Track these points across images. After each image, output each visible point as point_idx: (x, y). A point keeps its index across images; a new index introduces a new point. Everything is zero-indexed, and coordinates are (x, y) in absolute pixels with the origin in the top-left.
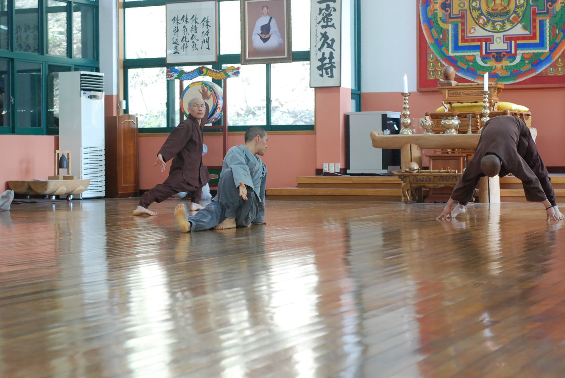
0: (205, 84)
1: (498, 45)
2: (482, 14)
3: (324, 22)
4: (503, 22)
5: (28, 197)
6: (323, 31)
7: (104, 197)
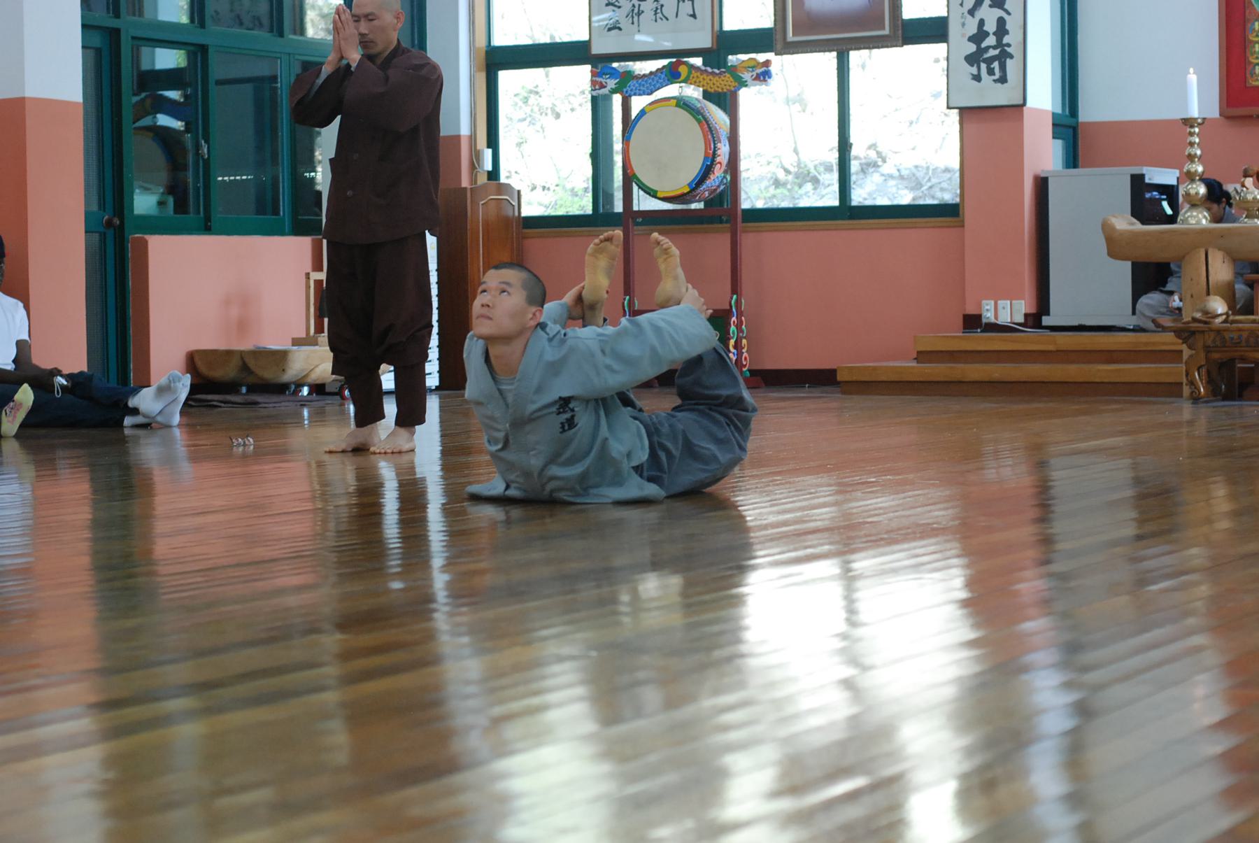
0: (683, 103)
5: (244, 390)
7: (437, 388)
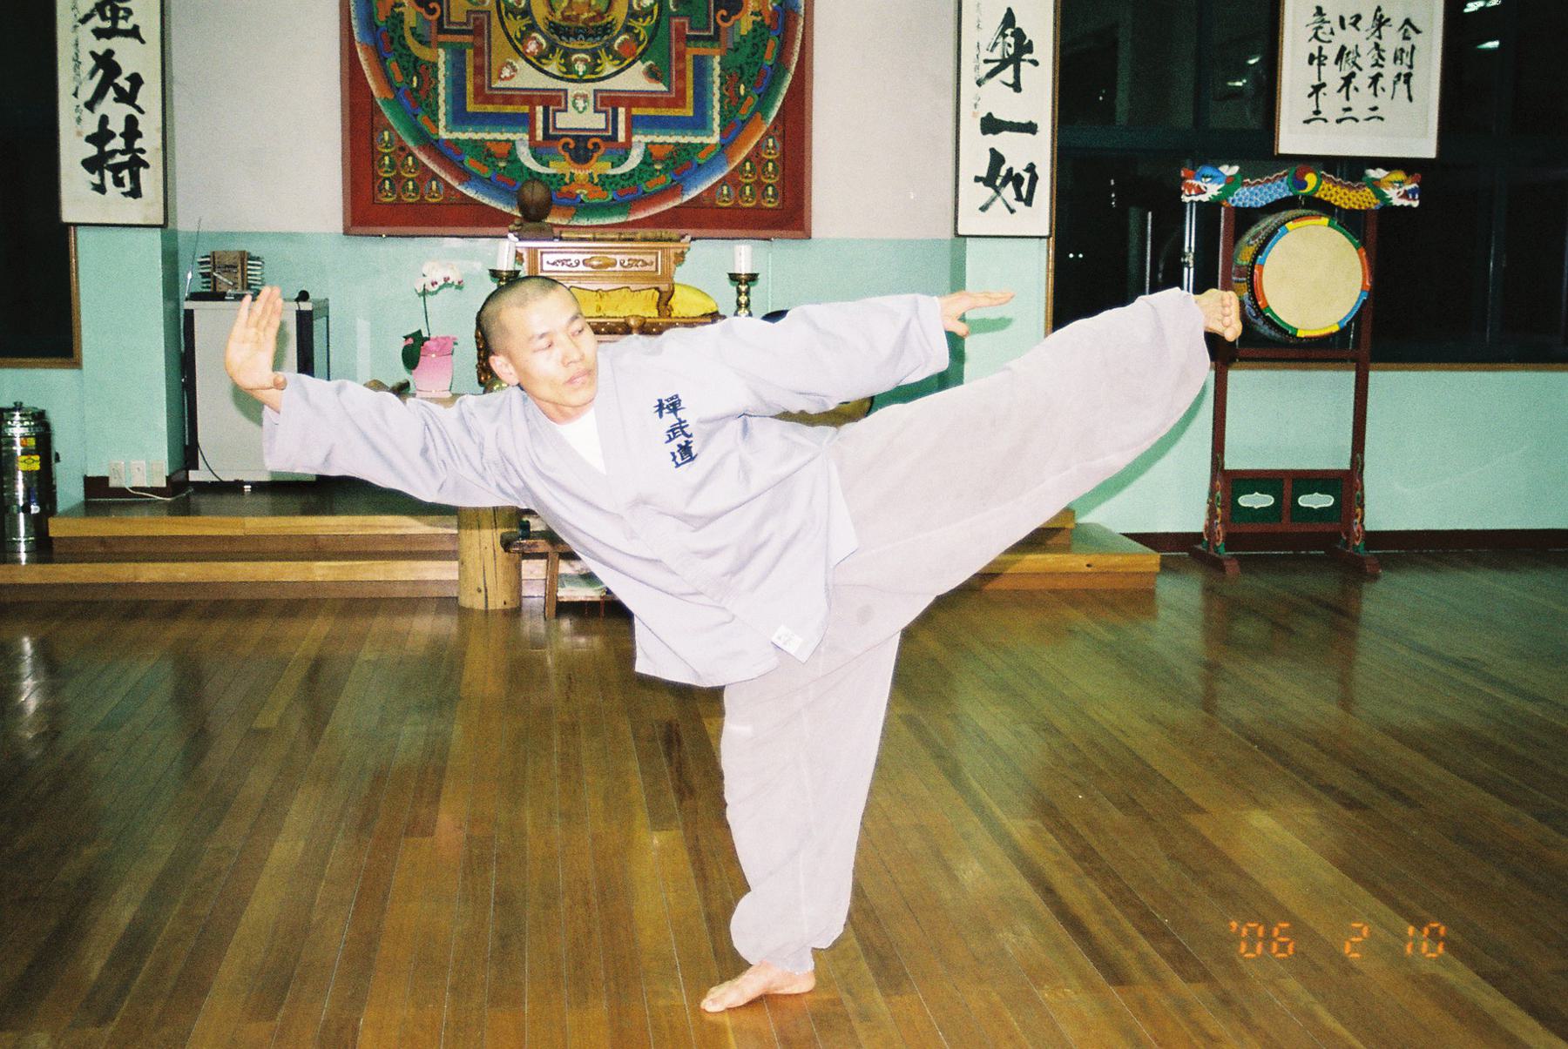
1: (580, 117)
2: (532, 27)
3: (104, 18)
4: (595, 55)
6: (101, 46)
